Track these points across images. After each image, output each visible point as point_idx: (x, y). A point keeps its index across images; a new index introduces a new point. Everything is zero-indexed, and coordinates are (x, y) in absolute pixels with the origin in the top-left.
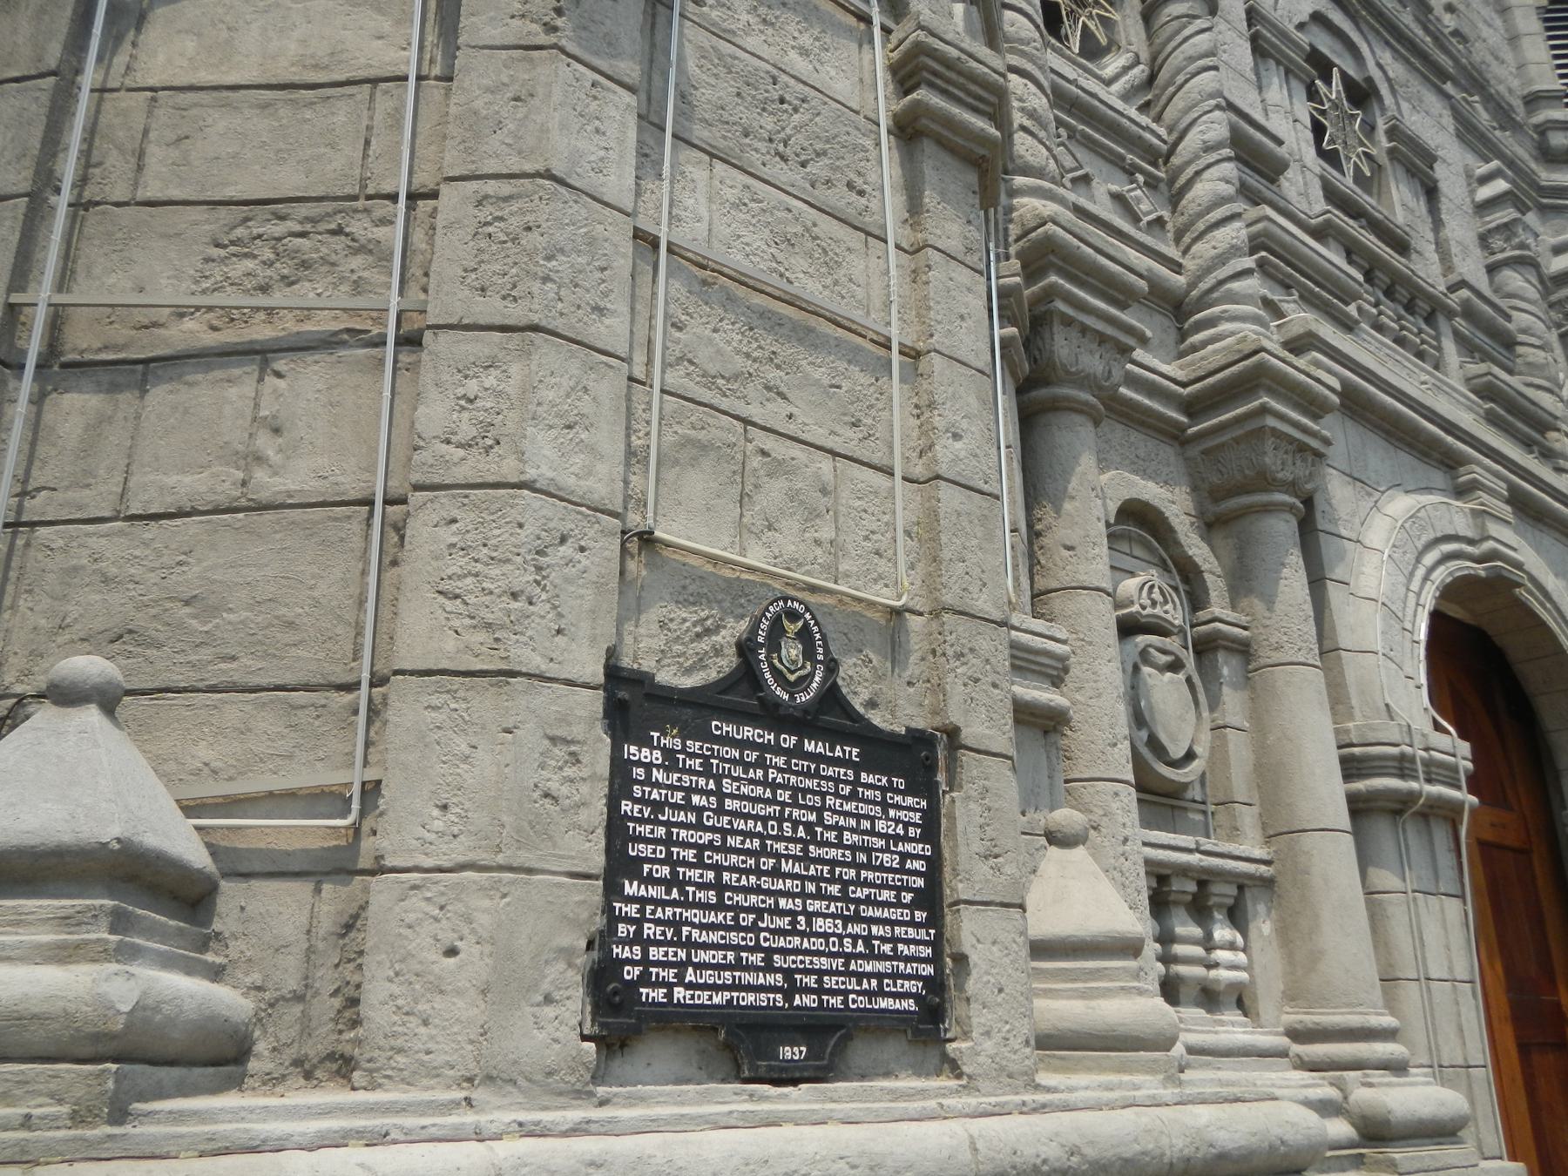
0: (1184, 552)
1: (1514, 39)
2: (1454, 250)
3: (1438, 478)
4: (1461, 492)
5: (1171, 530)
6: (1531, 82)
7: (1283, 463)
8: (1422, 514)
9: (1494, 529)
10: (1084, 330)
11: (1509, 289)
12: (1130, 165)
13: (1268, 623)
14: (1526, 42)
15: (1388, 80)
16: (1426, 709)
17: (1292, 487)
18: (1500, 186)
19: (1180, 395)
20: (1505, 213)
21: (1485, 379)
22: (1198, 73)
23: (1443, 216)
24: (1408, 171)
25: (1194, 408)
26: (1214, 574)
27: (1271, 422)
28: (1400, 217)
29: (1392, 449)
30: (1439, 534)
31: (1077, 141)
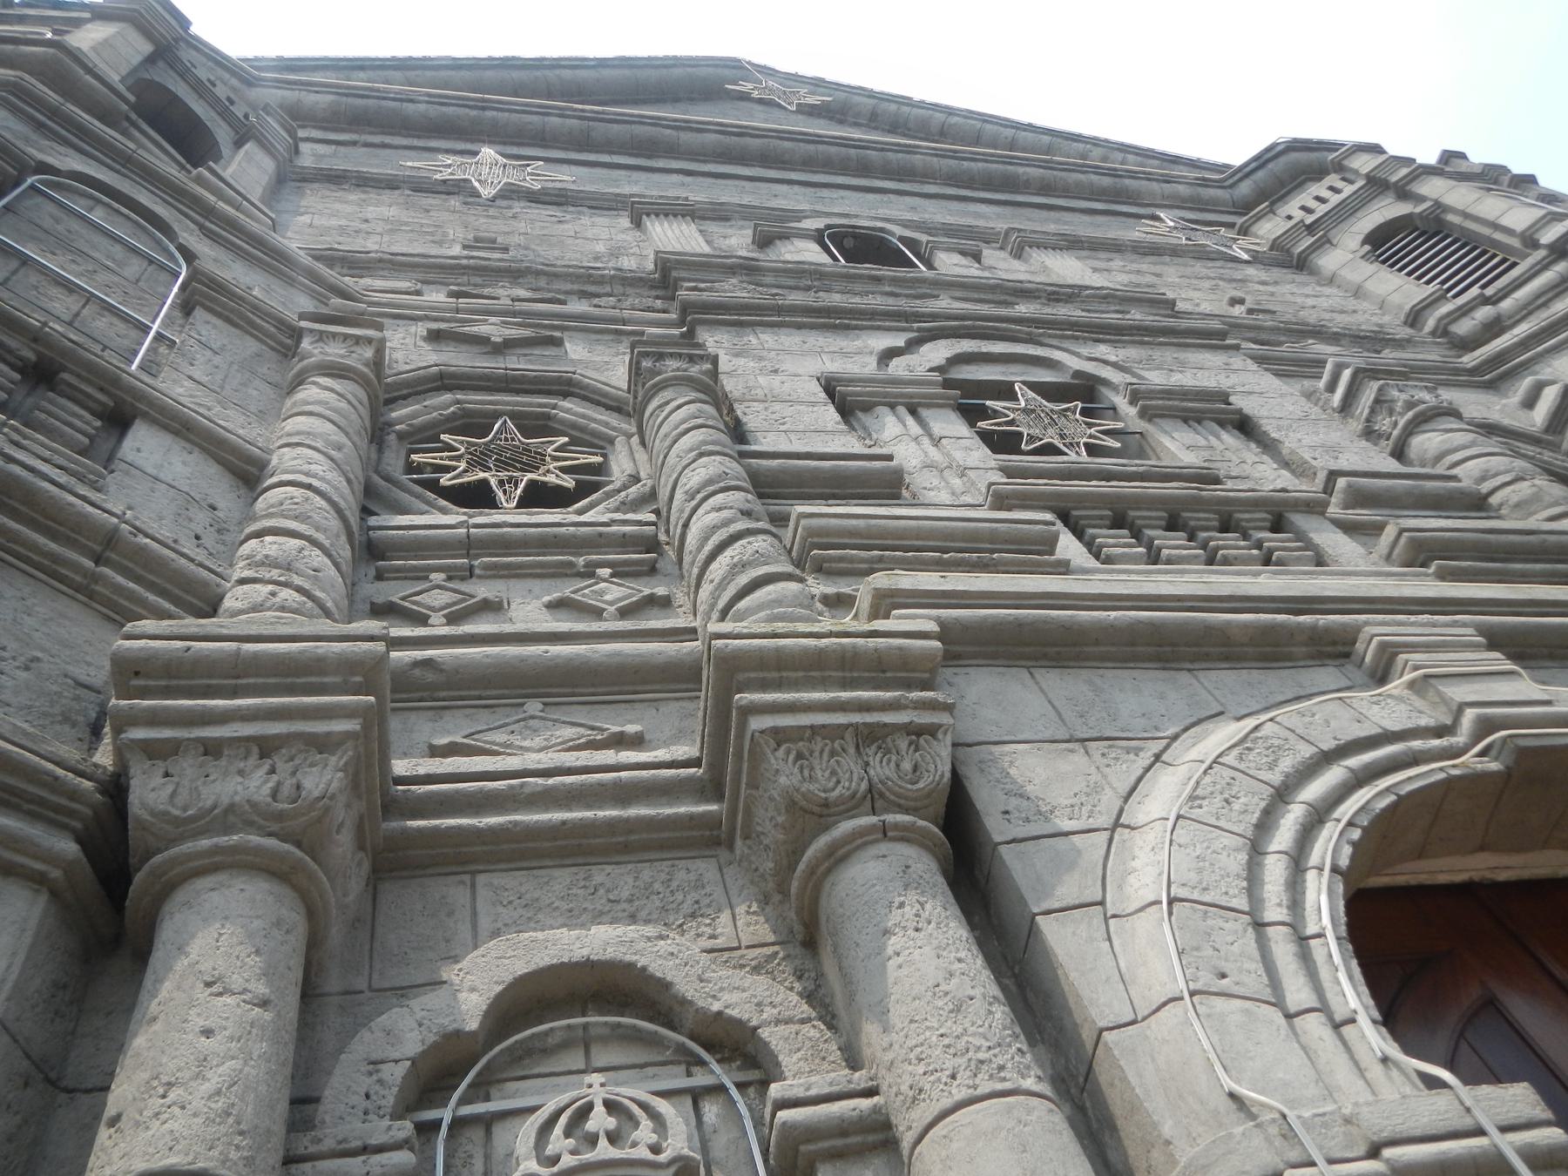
0: (702, 1013)
1: (1358, 292)
2: (1307, 456)
3: (1326, 676)
4: (1381, 676)
5: (665, 985)
6: (1400, 307)
7: (833, 773)
8: (1269, 729)
9: (1460, 692)
10: (212, 749)
11: (1431, 453)
12: (584, 566)
13: (889, 1056)
14: (1370, 286)
15: (1115, 365)
16: (1385, 1060)
17: (873, 798)
18: (1347, 374)
19: (690, 779)
20: (1368, 391)
21: (1403, 540)
22: (675, 442)
23: (1273, 435)
24: (1185, 421)
25: (712, 788)
26: (788, 1021)
27: (757, 723)
28: (1189, 459)
29: (1184, 677)
30: (1328, 744)
31: (480, 577)
